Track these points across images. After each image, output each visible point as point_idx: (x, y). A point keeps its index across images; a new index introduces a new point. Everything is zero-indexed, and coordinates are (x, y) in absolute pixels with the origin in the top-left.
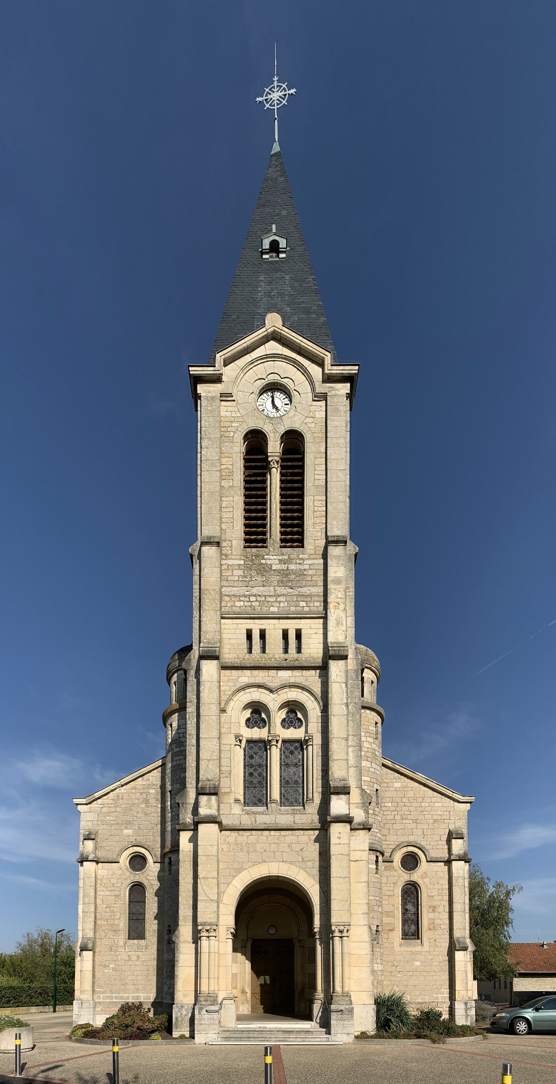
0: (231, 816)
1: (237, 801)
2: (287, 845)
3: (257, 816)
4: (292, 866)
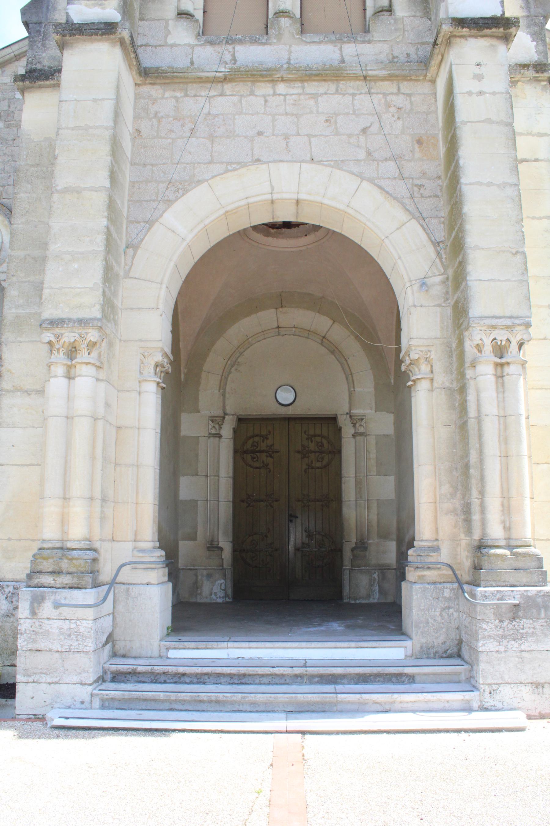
0: (166, 49)
1: (183, 14)
2: (323, 118)
3: (238, 47)
4: (337, 172)
